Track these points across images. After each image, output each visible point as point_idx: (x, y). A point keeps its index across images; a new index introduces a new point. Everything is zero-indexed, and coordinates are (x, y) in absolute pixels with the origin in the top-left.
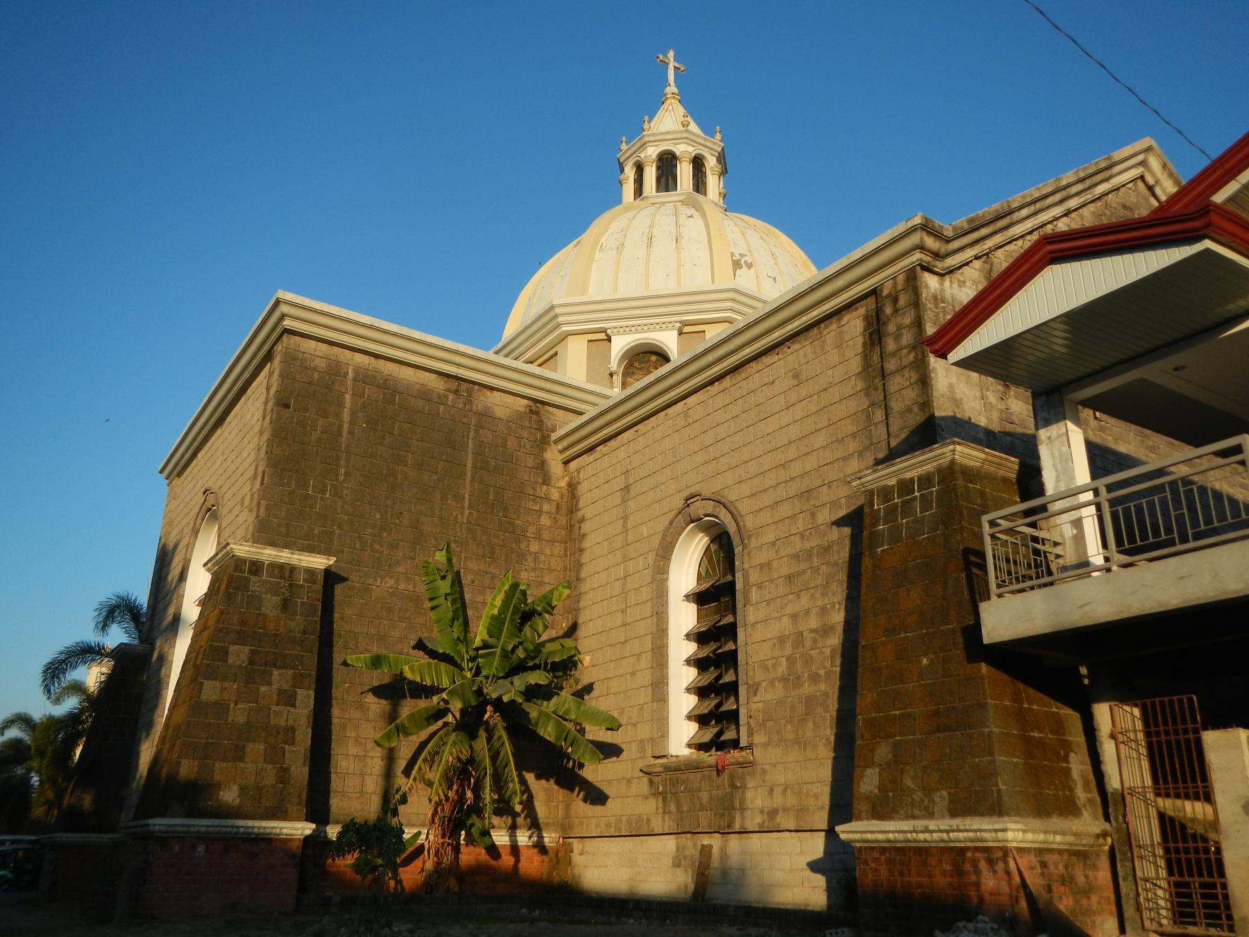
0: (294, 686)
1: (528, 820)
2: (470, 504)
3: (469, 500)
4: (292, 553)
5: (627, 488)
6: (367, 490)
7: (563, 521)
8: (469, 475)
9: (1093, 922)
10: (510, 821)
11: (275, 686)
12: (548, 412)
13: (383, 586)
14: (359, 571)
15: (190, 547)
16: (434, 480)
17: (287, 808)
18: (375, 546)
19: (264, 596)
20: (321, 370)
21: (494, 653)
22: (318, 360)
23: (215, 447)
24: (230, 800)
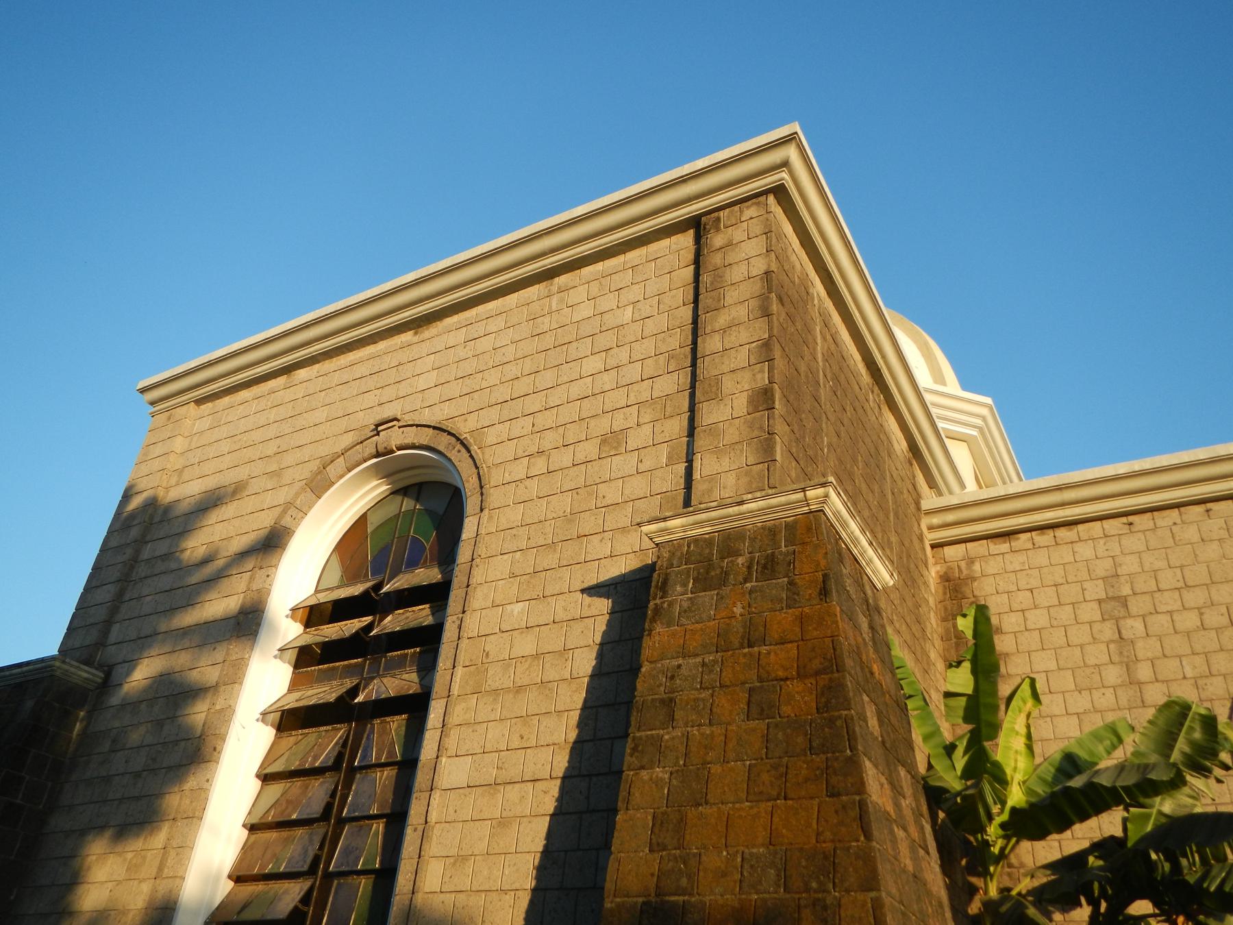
5: (1123, 602)
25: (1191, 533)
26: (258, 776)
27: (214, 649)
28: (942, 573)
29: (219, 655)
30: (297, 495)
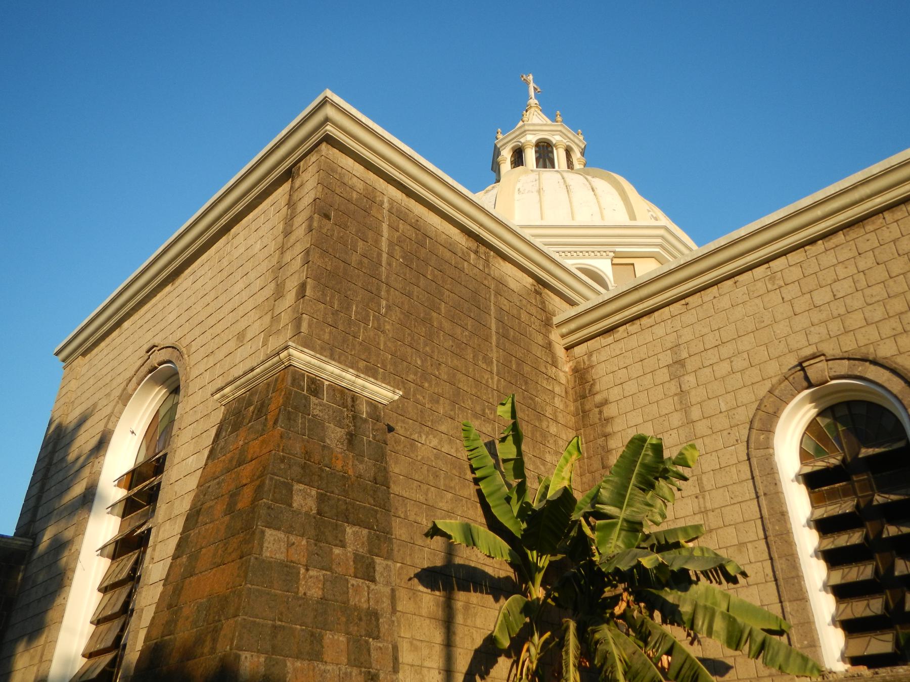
0: (370, 552)
2: (498, 370)
3: (497, 366)
4: (357, 376)
5: (681, 363)
6: (407, 330)
7: (572, 408)
8: (494, 338)
12: (549, 296)
13: (428, 444)
14: (403, 421)
15: (114, 417)
16: (465, 335)
18: (418, 396)
20: (359, 191)
21: (615, 524)
23: (160, 306)
25: (725, 302)
26: (100, 590)
27: (75, 514)
28: (572, 368)
29: (75, 519)
30: (115, 406)
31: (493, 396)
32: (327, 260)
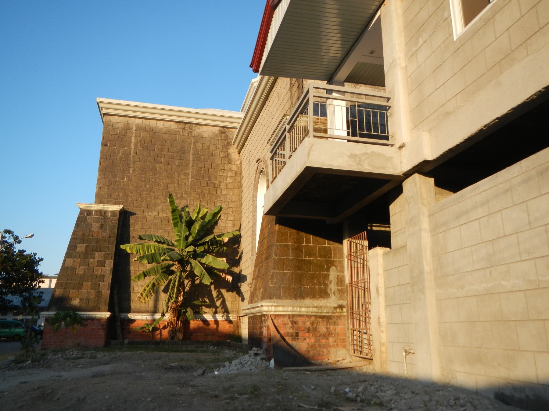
1: (223, 309)
3: (191, 175)
6: (143, 176)
9: (329, 351)
10: (214, 310)
11: (96, 259)
12: (230, 131)
13: (151, 215)
14: (140, 210)
16: (174, 168)
17: (100, 307)
19: (93, 223)
20: (121, 128)
22: (119, 124)
24: (76, 304)
31: (188, 188)
32: (106, 162)
